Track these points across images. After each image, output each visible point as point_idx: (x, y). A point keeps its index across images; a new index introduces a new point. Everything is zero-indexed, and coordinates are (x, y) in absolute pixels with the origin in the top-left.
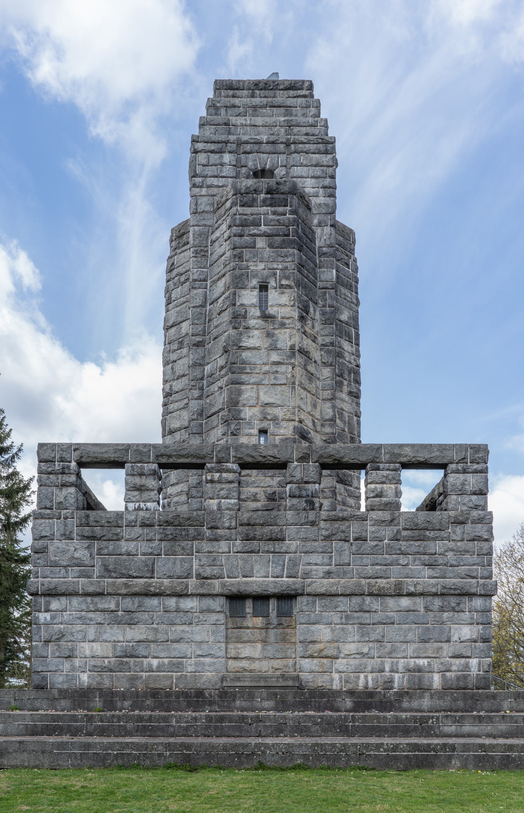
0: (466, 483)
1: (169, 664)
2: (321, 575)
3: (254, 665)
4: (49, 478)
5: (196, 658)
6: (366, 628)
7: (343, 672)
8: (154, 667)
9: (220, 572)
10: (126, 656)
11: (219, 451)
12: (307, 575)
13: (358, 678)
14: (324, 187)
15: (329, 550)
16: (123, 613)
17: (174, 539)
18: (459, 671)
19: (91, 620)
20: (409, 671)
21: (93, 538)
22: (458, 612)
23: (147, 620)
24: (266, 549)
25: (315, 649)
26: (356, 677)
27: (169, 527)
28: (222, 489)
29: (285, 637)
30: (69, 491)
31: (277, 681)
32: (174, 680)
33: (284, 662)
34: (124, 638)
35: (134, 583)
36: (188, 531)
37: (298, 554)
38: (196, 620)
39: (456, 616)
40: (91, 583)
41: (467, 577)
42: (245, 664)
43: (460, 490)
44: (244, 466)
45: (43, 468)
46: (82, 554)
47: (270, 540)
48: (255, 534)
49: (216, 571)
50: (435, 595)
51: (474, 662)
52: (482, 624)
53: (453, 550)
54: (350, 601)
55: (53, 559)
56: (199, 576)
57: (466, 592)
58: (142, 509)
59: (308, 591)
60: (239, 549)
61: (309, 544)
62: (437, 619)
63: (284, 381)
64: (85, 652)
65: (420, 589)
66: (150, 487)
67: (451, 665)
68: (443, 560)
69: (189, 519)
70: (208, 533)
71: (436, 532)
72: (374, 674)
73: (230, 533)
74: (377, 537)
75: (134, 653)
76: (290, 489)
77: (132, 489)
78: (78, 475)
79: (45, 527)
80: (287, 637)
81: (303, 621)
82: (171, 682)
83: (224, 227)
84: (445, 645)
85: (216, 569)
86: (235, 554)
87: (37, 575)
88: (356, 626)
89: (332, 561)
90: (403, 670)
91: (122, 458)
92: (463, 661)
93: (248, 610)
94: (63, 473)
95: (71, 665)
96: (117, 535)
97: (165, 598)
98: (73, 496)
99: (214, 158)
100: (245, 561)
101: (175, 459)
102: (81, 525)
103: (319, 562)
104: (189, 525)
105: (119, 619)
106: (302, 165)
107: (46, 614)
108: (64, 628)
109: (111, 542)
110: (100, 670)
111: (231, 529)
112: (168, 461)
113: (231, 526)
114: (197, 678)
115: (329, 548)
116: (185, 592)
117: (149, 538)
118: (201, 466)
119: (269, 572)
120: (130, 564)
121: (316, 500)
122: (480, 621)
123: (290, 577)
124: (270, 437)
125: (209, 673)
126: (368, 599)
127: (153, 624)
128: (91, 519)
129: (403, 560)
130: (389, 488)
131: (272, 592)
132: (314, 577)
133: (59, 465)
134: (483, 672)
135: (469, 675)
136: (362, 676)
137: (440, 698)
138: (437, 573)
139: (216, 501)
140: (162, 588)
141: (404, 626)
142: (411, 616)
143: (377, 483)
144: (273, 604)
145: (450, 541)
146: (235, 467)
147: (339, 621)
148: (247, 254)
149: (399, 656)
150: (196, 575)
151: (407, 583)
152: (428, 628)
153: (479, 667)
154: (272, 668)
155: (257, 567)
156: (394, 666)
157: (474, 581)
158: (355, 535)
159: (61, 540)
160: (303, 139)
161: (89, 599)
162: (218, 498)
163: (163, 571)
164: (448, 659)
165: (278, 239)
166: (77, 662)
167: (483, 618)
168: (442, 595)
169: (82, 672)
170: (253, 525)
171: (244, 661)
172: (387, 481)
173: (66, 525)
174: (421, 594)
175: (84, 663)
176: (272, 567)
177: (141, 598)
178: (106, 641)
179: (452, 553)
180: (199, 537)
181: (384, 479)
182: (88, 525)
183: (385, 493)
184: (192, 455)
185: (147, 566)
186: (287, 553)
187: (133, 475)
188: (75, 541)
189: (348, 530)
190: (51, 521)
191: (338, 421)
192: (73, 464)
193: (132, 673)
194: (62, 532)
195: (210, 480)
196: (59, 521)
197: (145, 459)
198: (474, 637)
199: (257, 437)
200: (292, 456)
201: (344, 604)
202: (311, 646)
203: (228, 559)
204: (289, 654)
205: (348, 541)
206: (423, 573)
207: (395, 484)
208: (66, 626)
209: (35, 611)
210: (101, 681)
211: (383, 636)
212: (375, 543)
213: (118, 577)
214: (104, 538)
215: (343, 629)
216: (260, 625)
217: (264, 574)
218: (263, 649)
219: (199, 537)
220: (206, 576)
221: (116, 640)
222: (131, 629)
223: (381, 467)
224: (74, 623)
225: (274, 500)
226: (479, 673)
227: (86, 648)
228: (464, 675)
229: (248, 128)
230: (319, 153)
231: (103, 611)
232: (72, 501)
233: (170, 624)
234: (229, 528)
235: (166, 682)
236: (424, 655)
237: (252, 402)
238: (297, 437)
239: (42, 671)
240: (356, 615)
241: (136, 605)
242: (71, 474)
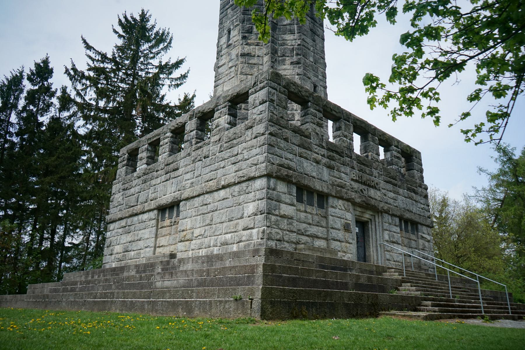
50: (235, 184)
69: (149, 169)
170: (170, 164)
174: (229, 186)
179: (245, 151)
236: (229, 231)
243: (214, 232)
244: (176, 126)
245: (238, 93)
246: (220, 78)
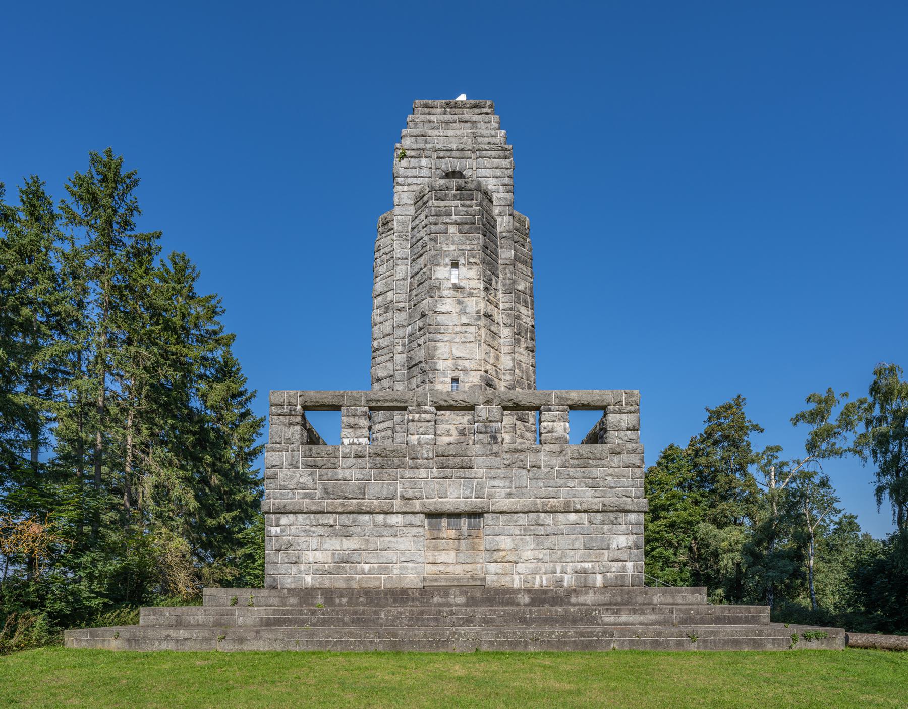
2: (504, 496)
10: (343, 562)
13: (534, 578)
14: (504, 185)
19: (314, 532)
20: (576, 572)
21: (316, 466)
28: (421, 427)
33: (474, 566)
37: (484, 479)
38: (401, 533)
40: (314, 503)
42: (442, 568)
44: (439, 408)
46: (306, 479)
47: (461, 468)
50: (597, 511)
53: (611, 475)
58: (356, 444)
60: (435, 476)
63: (472, 339)
65: (585, 507)
69: (394, 451)
72: (547, 575)
73: (429, 463)
75: (349, 559)
78: (303, 416)
83: (422, 217)
84: (606, 552)
88: (532, 537)
93: (443, 525)
96: (335, 464)
99: (414, 162)
102: (305, 456)
103: (501, 485)
104: (394, 456)
106: (486, 168)
116: (391, 510)
118: (404, 409)
121: (498, 435)
123: (478, 498)
124: (461, 384)
126: (543, 515)
128: (314, 451)
129: (571, 483)
136: (538, 577)
137: (602, 594)
139: (416, 437)
141: (572, 537)
142: (578, 529)
148: (441, 239)
152: (592, 538)
155: (450, 490)
160: (486, 147)
161: (312, 516)
165: (466, 226)
177: (354, 515)
180: (402, 466)
182: (311, 456)
185: (360, 489)
187: (348, 416)
191: (516, 370)
197: (357, 403)
199: (450, 385)
201: (523, 519)
203: (426, 484)
206: (587, 494)
215: (522, 539)
216: (453, 537)
218: (457, 556)
223: (552, 409)
225: (464, 435)
227: (310, 556)
229: (442, 138)
230: (499, 158)
234: (427, 459)
237: (446, 356)
238: (483, 384)
240: (532, 528)
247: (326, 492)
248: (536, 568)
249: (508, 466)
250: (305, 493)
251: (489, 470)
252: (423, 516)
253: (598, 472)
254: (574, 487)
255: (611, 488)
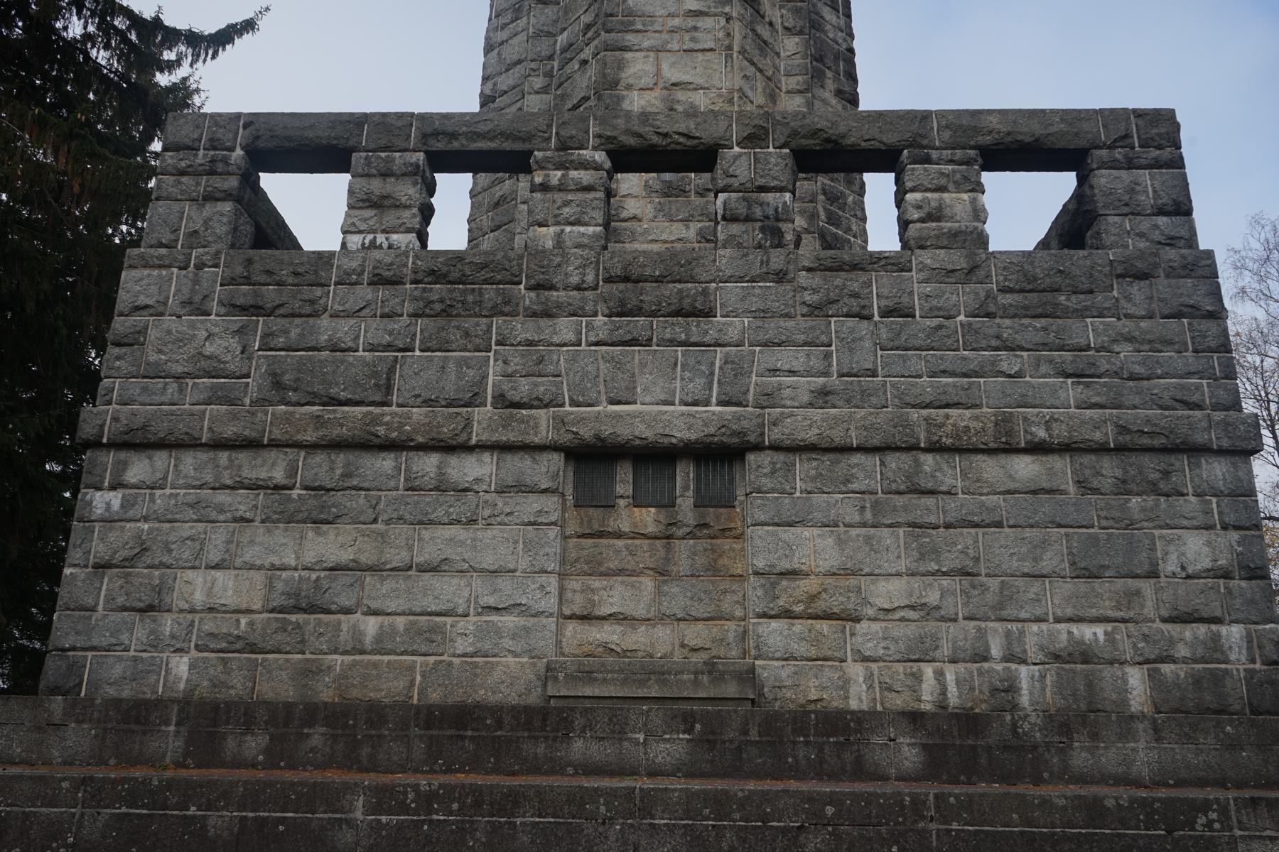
0: (1138, 188)
1: (407, 630)
2: (806, 398)
3: (634, 638)
4: (180, 183)
5: (479, 614)
6: (929, 536)
7: (875, 661)
8: (368, 640)
9: (554, 389)
10: (297, 609)
11: (564, 123)
12: (768, 398)
13: (918, 677)
15: (824, 338)
16: (304, 492)
17: (446, 313)
18: (1195, 661)
22: (1168, 496)
23: (362, 512)
24: (668, 336)
25: (798, 593)
26: (913, 674)
27: (438, 286)
28: (567, 203)
29: (715, 561)
30: (218, 209)
31: (696, 683)
32: (418, 678)
33: (715, 629)
34: (297, 558)
35: (338, 416)
36: (481, 294)
37: (746, 348)
38: (487, 512)
39: (1163, 506)
40: (234, 417)
41: (1177, 405)
42: (609, 634)
43: (1126, 205)
45: (170, 161)
46: (224, 347)
47: (678, 313)
48: (641, 301)
49: (542, 389)
50: (1101, 449)
51: (1233, 633)
52: (1237, 528)
53: (1129, 339)
54: (882, 463)
55: (153, 357)
56: (502, 401)
57: (1183, 443)
58: (381, 247)
59: (773, 437)
61: (771, 324)
62: (1116, 514)
64: (192, 594)
65: (1061, 433)
66: (404, 199)
67: (1172, 642)
68: (1109, 362)
69: (484, 266)
70: (528, 298)
71: (1082, 296)
72: (961, 667)
73: (583, 299)
74: (939, 309)
76: (725, 203)
77: (361, 204)
79: (149, 285)
80: (720, 562)
81: (763, 518)
82: (407, 684)
84: (1146, 586)
85: (542, 384)
86: (593, 348)
87: (107, 398)
88: (901, 531)
89: (830, 365)
90: (1041, 657)
91: (348, 139)
92: (1202, 629)
93: (620, 489)
94: (212, 173)
95: (152, 632)
96: (312, 302)
97: (411, 454)
98: (225, 220)
100: (617, 363)
101: (465, 142)
103: (797, 366)
104: (486, 282)
105: (291, 507)
107: (112, 494)
108: (151, 531)
109: (298, 321)
110: (224, 645)
111: (585, 289)
112: (449, 147)
113: (583, 281)
114: (478, 671)
115: (823, 333)
116: (462, 439)
117: (387, 310)
119: (674, 392)
120: (334, 372)
121: (785, 227)
122: (1231, 518)
125: (511, 659)
126: (928, 460)
127: (375, 521)
130: (957, 201)
131: (682, 440)
132: (788, 403)
133: (205, 155)
134: (1263, 663)
135: (1226, 672)
136: (928, 671)
138: (1098, 394)
139: (552, 230)
140: (407, 428)
141: (1028, 533)
142: (1046, 507)
143: (927, 190)
144: (684, 474)
145: (1119, 319)
146: (600, 157)
147: (857, 518)
149: (1023, 615)
150: (493, 397)
151: (1025, 419)
152: (1095, 540)
153: (1249, 649)
154: (683, 645)
155: (643, 380)
156: (1015, 644)
157: (1198, 414)
158: (884, 303)
159: (179, 317)
161: (223, 457)
162: (558, 223)
163: (414, 388)
164: (1158, 624)
166: (168, 624)
167: (1236, 511)
168: (1120, 449)
169: (176, 651)
170: (637, 281)
171: (607, 627)
172: (951, 186)
173: (196, 281)
174: (1066, 448)
175: (185, 625)
176: (682, 379)
177: (351, 456)
178: (252, 567)
180: (505, 308)
181: (943, 181)
182: (247, 280)
183: (947, 212)
184: (502, 134)
185: (375, 374)
186: (720, 345)
187: (368, 175)
188: (212, 317)
189: (868, 290)
190: (164, 272)
192: (239, 152)
193: (308, 656)
194: (185, 298)
195: (541, 184)
196: (184, 272)
197: (399, 142)
198: (1222, 562)
200: (728, 134)
201: (867, 473)
202: (784, 583)
203: (574, 359)
204: (725, 606)
205: (869, 318)
206: (1062, 395)
207: (970, 191)
208: (157, 525)
209: (88, 487)
210: (223, 677)
211: (977, 560)
212: (936, 321)
213: (303, 401)
214: (282, 311)
215: (868, 539)
216: (651, 529)
217: (662, 397)
218: (659, 592)
219: (507, 309)
220: (517, 399)
221: (277, 563)
222: (318, 533)
224: (177, 516)
226: (1251, 666)
228: (1212, 673)
231: (255, 486)
232: (221, 229)
233: (421, 523)
234: (578, 288)
235: (396, 683)
236: (1094, 612)
239: (73, 649)
240: (900, 501)
241: (338, 472)
242: (229, 174)
243: (1000, 606)
244: (656, 139)
245: (1036, 140)
246: (640, 27)
247: (278, 385)
248: (921, 640)
249: (816, 310)
250: (213, 387)
251: (759, 323)
252: (557, 460)
253: (1091, 331)
254: (1019, 375)
255: (1132, 378)
